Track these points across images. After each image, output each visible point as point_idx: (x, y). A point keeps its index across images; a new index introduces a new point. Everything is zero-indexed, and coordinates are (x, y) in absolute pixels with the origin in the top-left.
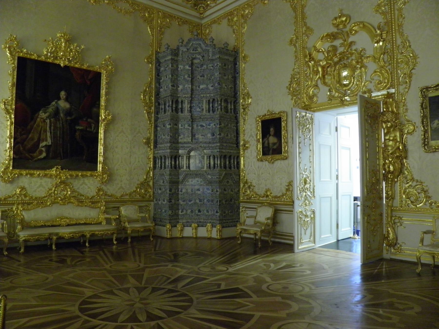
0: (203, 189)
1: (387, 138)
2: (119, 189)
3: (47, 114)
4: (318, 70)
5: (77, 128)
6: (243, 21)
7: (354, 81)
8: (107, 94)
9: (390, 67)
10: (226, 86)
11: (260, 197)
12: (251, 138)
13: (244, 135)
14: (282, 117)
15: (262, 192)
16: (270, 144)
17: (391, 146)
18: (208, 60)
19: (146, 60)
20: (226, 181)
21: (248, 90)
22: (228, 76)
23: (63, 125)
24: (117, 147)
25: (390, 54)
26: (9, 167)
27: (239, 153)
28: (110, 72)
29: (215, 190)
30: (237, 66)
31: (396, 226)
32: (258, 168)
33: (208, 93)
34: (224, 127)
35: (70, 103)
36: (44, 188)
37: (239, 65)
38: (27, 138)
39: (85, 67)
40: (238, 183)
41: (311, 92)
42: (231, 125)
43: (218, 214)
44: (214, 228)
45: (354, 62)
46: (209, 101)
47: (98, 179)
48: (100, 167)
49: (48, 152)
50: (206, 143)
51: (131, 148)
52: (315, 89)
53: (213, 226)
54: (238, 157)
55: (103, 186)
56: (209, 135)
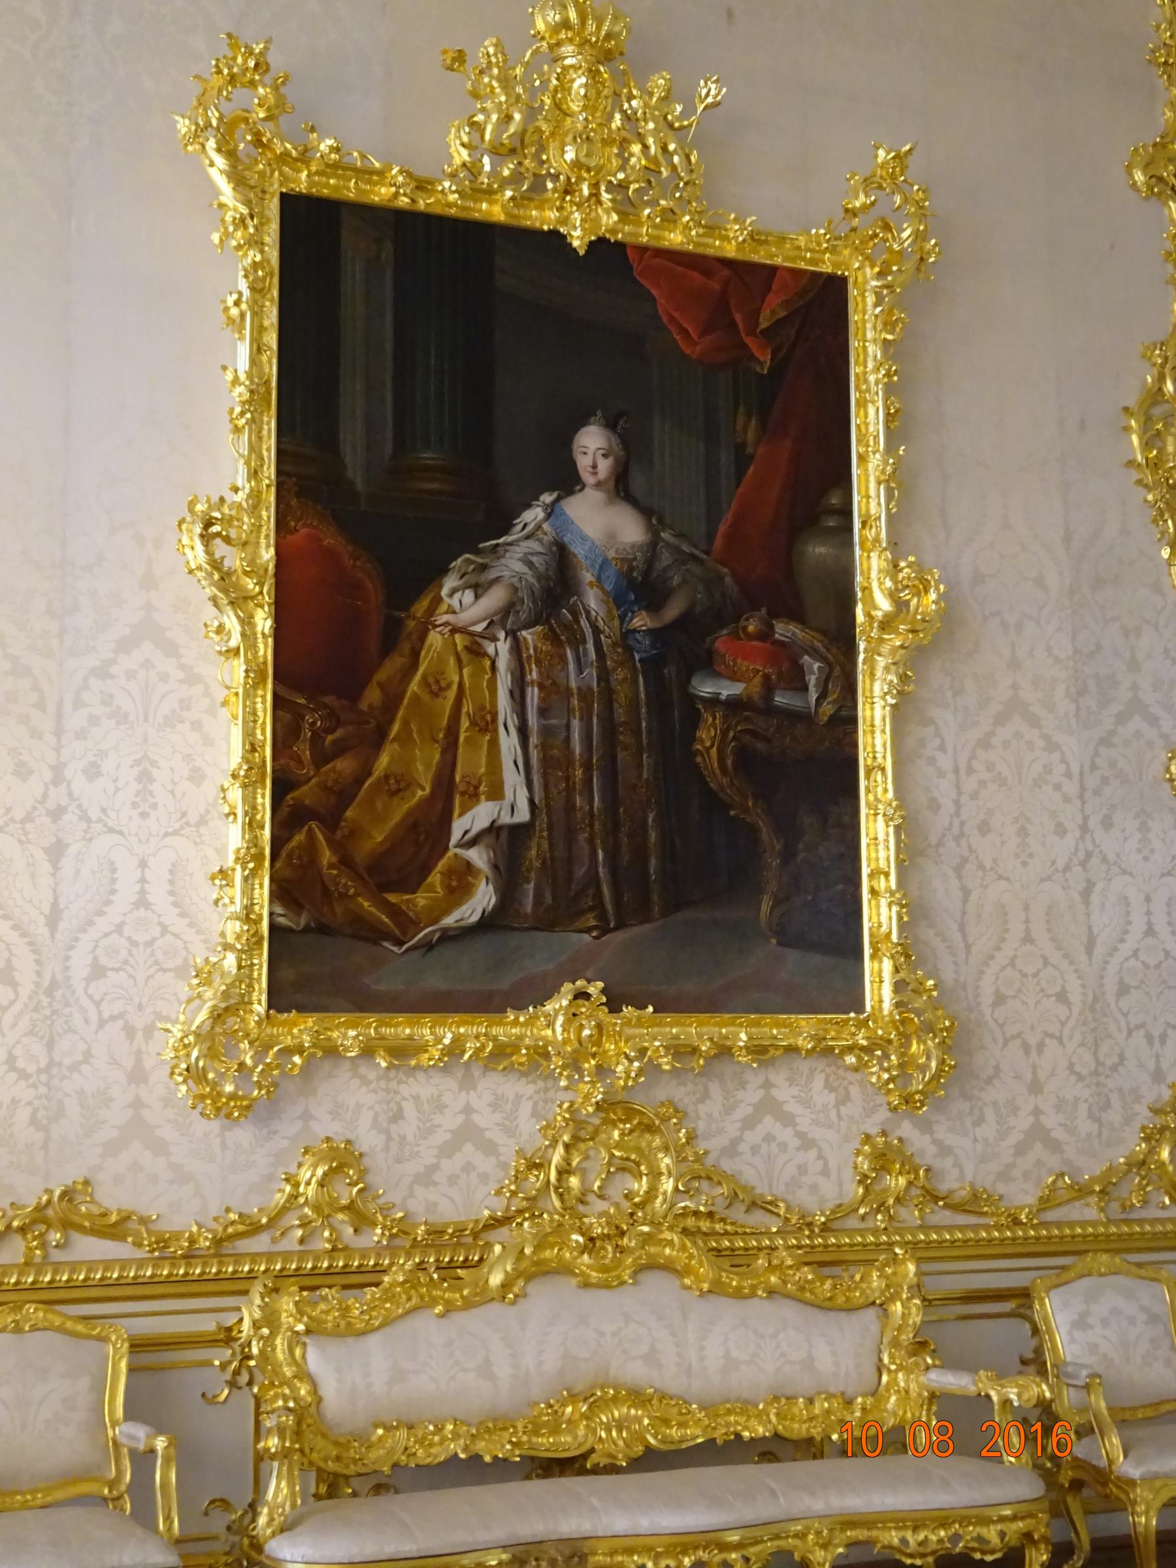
2: (1021, 1149)
3: (494, 599)
5: (705, 688)
8: (898, 428)
19: (1139, 176)
23: (604, 675)
24: (984, 828)
26: (245, 1002)
28: (909, 266)
35: (646, 512)
36: (490, 1149)
38: (359, 781)
39: (730, 245)
47: (876, 1074)
48: (879, 981)
49: (508, 878)
51: (1084, 828)
55: (906, 1129)
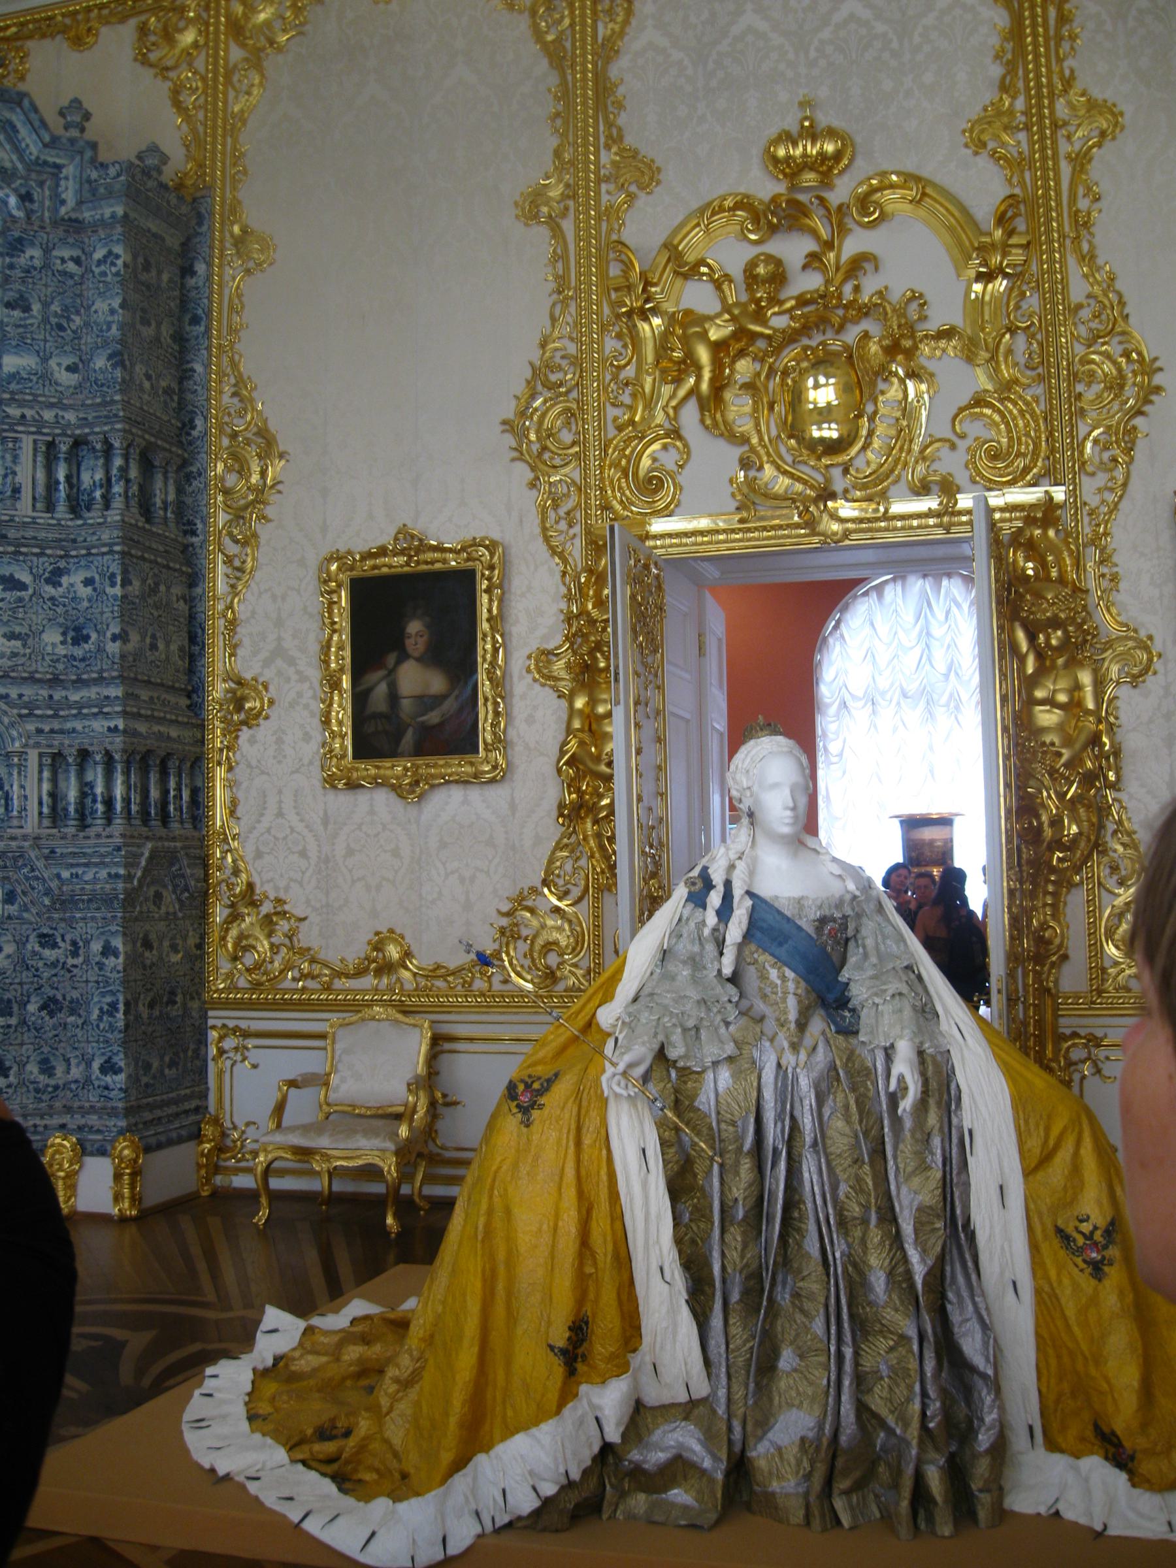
0: (21, 943)
1: (1039, 694)
4: (689, 363)
6: (236, 54)
7: (871, 433)
9: (1039, 390)
10: (149, 377)
11: (340, 975)
12: (279, 662)
13: (235, 646)
14: (479, 567)
15: (354, 951)
16: (406, 704)
17: (1060, 728)
18: (55, 223)
20: (151, 892)
21: (260, 413)
22: (159, 324)
25: (1039, 337)
27: (202, 742)
29: (96, 947)
30: (191, 282)
31: (1076, 1077)
32: (326, 821)
33: (52, 406)
34: (143, 597)
37: (209, 278)
40: (200, 901)
41: (646, 462)
42: (168, 588)
43: (121, 1077)
44: (90, 1161)
45: (874, 348)
46: (51, 445)
50: (32, 679)
52: (665, 447)
53: (83, 1150)
54: (196, 763)
56: (52, 637)
